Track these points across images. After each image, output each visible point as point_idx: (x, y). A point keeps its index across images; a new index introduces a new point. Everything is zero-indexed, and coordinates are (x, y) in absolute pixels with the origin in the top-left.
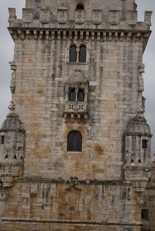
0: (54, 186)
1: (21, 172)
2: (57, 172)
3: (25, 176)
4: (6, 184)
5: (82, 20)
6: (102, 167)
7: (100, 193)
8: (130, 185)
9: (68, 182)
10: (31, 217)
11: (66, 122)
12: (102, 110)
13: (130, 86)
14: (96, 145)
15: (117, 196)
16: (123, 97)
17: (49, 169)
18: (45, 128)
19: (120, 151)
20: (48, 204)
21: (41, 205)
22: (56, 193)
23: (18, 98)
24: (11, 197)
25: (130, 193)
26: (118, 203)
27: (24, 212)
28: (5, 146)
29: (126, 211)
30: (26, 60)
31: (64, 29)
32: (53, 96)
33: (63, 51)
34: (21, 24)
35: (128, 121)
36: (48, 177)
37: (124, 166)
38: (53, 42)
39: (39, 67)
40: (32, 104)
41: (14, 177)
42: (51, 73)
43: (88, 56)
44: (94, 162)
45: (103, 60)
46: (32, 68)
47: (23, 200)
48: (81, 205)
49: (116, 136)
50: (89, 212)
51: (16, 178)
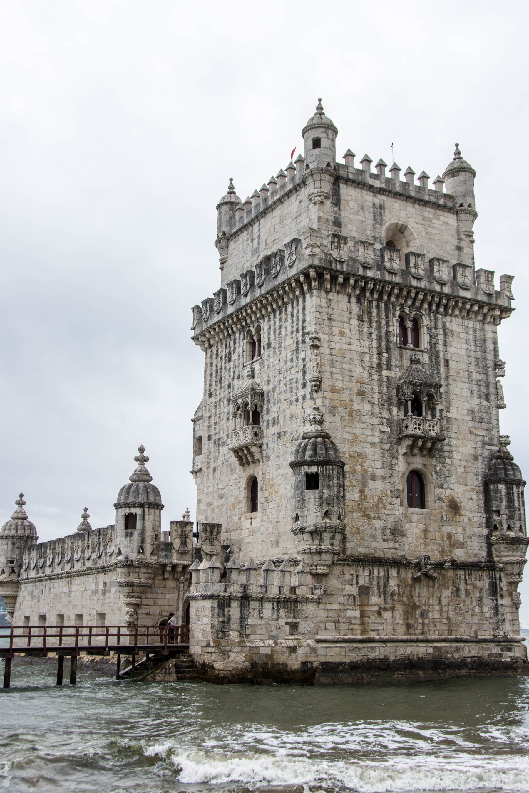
0: (394, 572)
1: (342, 545)
2: (397, 545)
3: (348, 552)
4: (322, 568)
5: (422, 273)
6: (461, 538)
7: (461, 585)
8: (501, 570)
9: (418, 565)
10: (363, 632)
11: (405, 454)
12: (453, 435)
13: (487, 397)
14: (450, 498)
15: (485, 589)
16: (479, 415)
17: (384, 540)
18: (374, 462)
19: (483, 510)
20: (388, 606)
21: (376, 608)
22: (398, 586)
23: (327, 402)
24: (328, 595)
25: (502, 584)
26: (488, 602)
27: (351, 623)
28: (323, 493)
29: (500, 617)
30: (336, 331)
31: (398, 284)
32: (382, 405)
33: (391, 323)
34: (330, 262)
35: (488, 458)
36: (384, 554)
37: (493, 538)
38: (374, 303)
39: (356, 347)
40: (350, 415)
41: (335, 554)
42: (376, 361)
43: (425, 338)
44: (448, 529)
45: (449, 349)
46: (346, 347)
47: (348, 599)
48: (437, 607)
49: (476, 483)
50: (448, 619)
51: (336, 557)
